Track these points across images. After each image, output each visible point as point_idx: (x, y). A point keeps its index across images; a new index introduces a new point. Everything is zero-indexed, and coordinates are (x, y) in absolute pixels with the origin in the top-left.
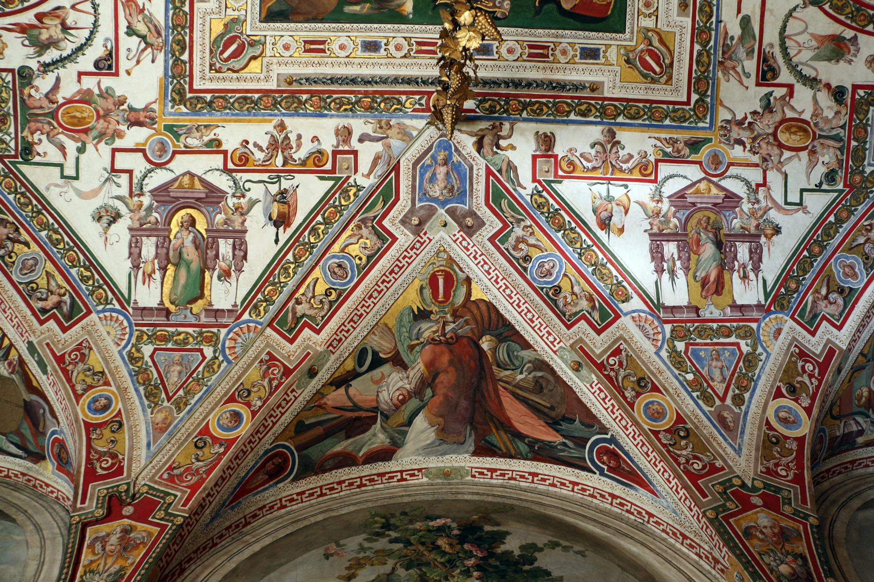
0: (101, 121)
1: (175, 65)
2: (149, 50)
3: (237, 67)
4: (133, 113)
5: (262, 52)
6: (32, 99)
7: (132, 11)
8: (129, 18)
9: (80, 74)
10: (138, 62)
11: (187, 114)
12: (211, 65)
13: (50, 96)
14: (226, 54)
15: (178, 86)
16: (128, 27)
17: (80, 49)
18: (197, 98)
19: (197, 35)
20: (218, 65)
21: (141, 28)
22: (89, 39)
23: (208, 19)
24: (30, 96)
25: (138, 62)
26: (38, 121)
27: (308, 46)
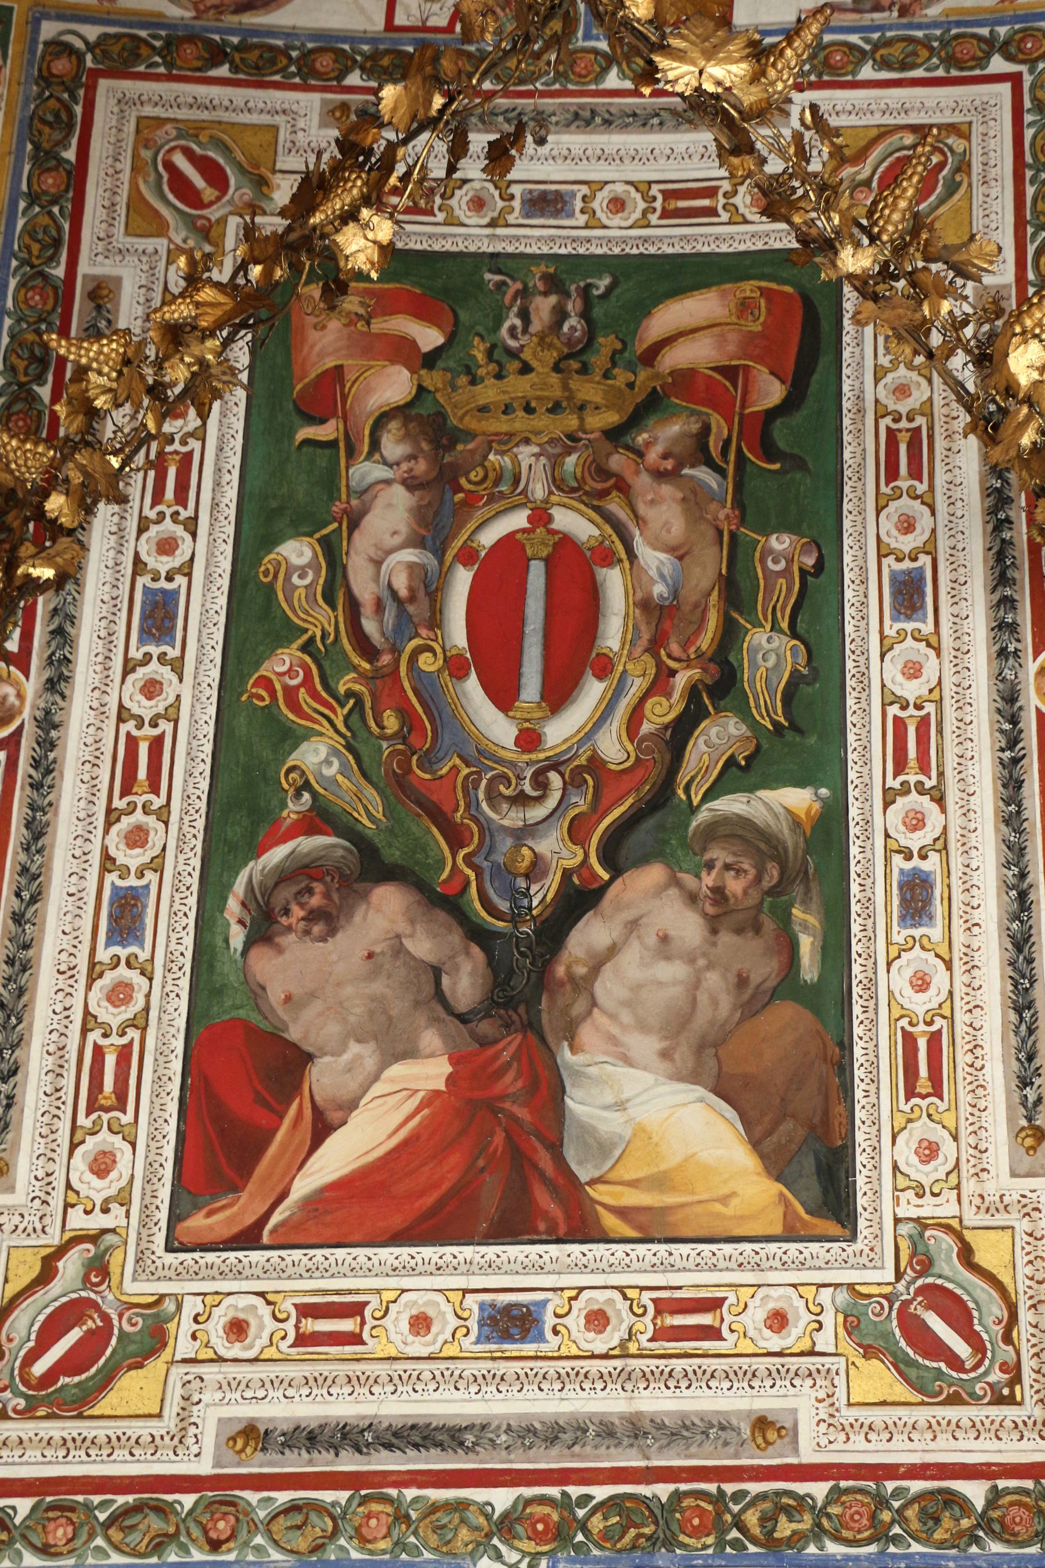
3: (997, 1310)
5: (948, 1228)
12: (999, 1400)
14: (961, 1348)
20: (997, 1376)
23: (849, 1415)
27: (923, 1084)
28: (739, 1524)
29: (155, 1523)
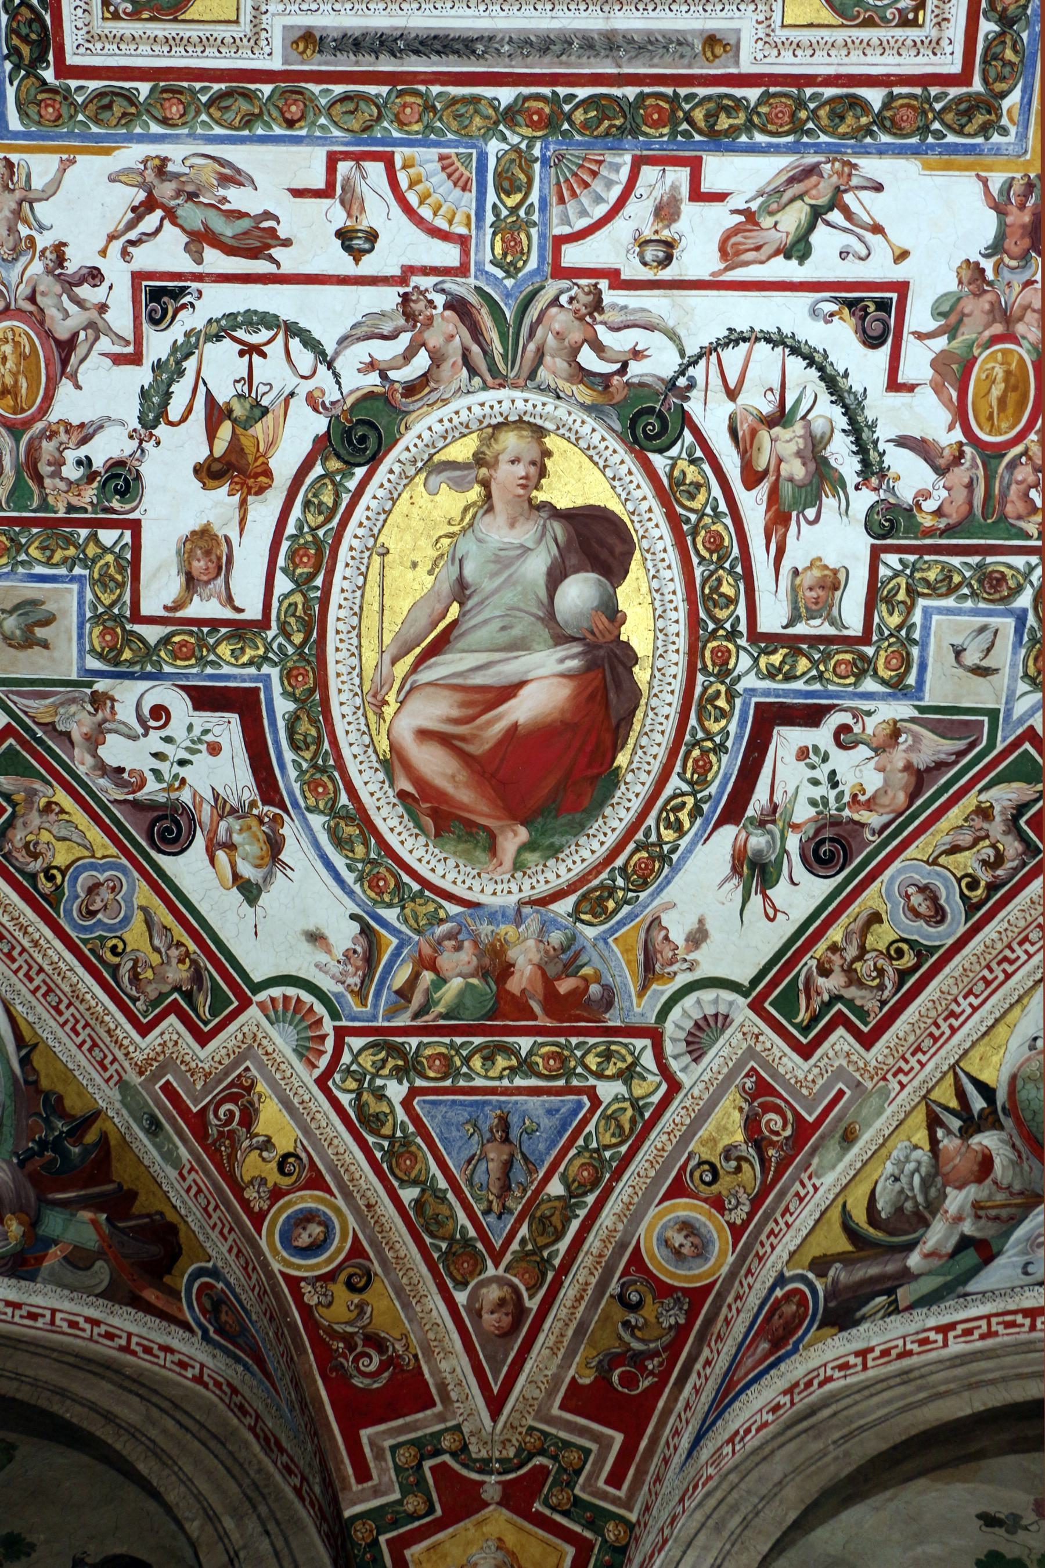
0: (1020, 328)
1: (894, 127)
2: (848, 198)
4: (1008, 243)
6: (947, 509)
7: (751, 243)
8: (767, 250)
9: (894, 385)
10: (877, 229)
11: (1027, 91)
13: (942, 462)
15: (949, 117)
16: (788, 257)
17: (831, 382)
18: (985, 61)
19: (822, 65)
21: (792, 218)
22: (810, 358)
23: (781, 34)
24: (939, 513)
25: (877, 229)
26: (1004, 495)
28: (689, 119)
29: (244, 106)
